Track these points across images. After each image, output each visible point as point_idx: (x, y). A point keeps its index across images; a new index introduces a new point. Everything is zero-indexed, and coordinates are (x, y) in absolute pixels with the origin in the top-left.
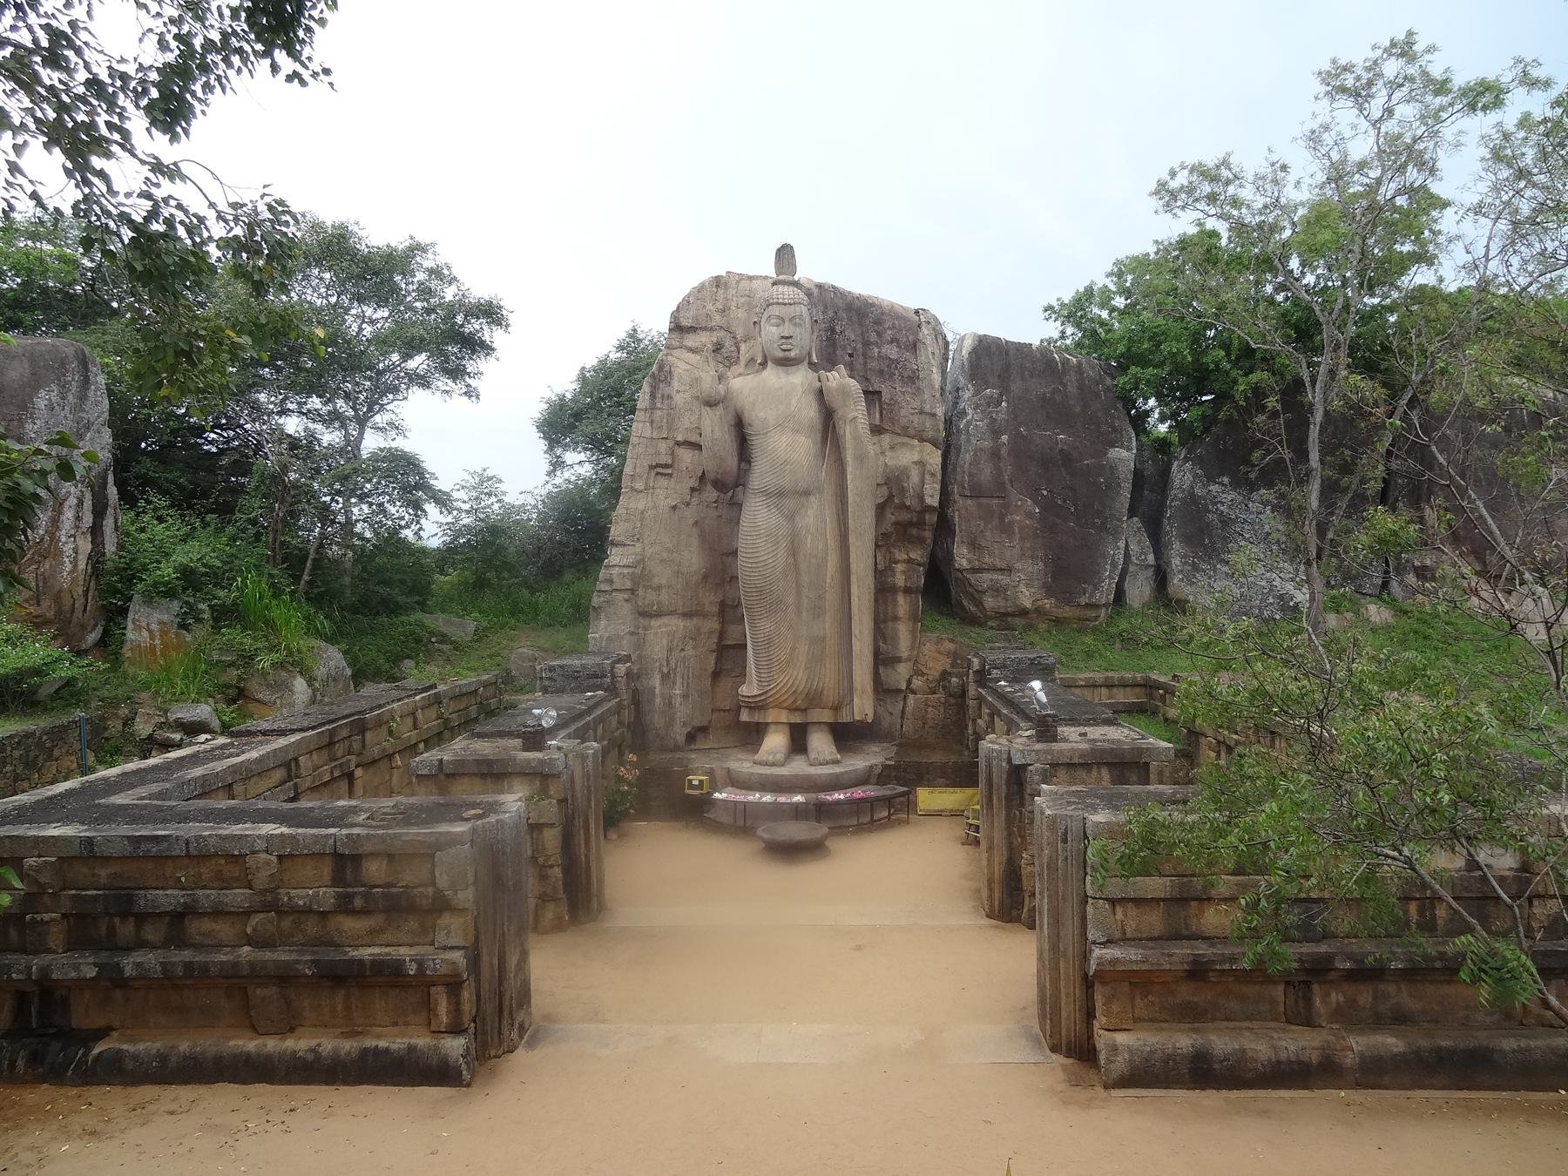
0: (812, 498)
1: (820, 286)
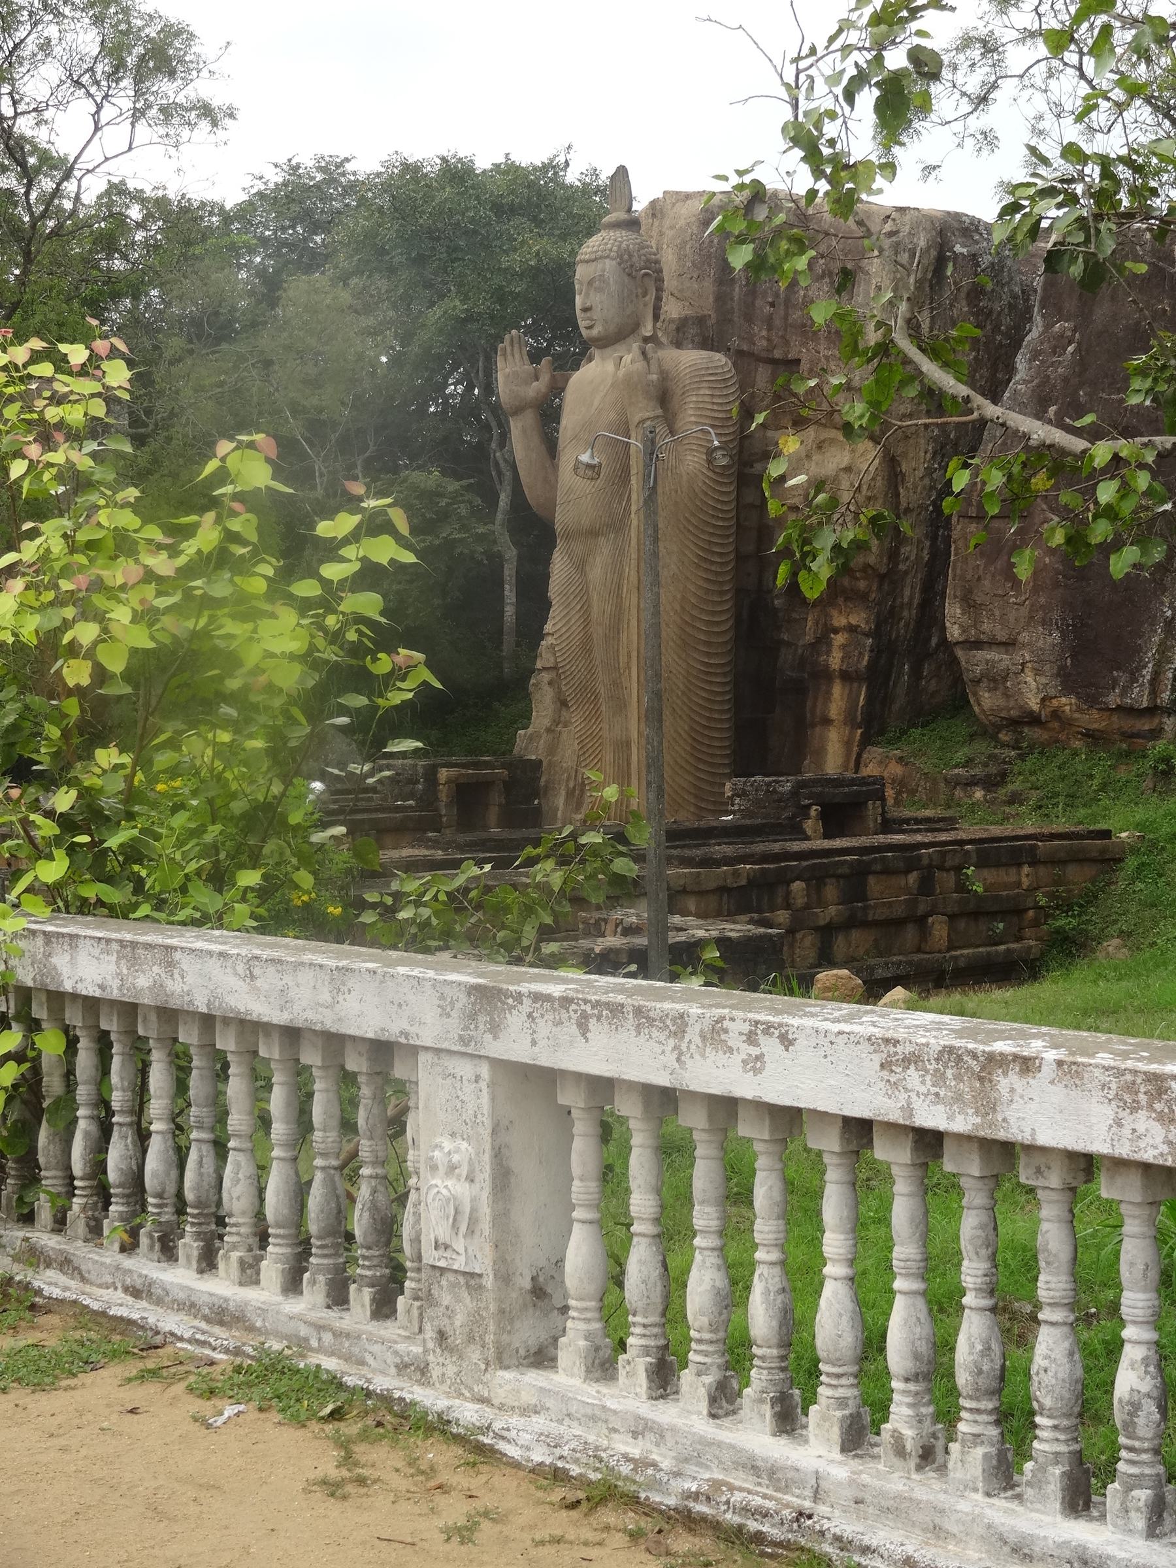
0: (602, 540)
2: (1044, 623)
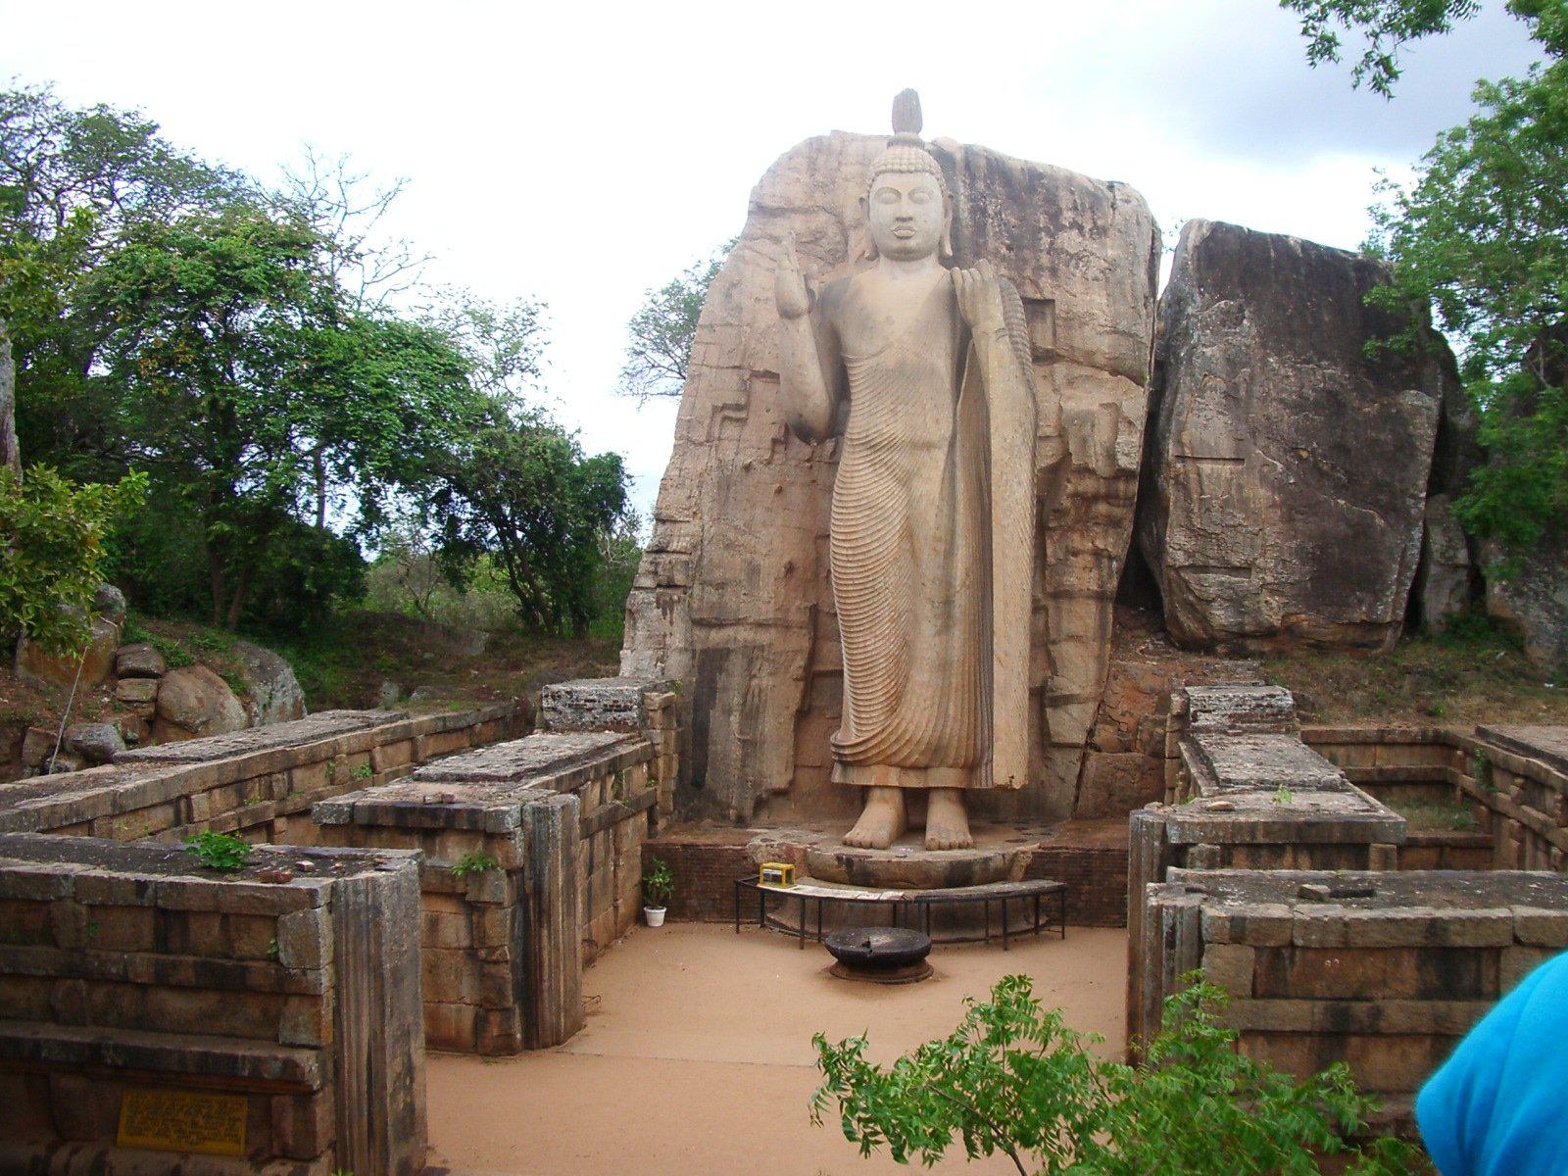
1: (969, 152)
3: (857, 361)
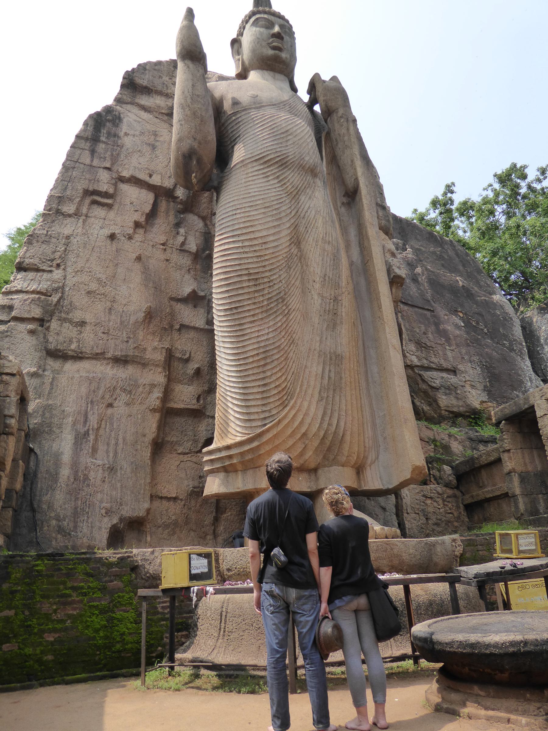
2: (471, 362)
3: (243, 110)
